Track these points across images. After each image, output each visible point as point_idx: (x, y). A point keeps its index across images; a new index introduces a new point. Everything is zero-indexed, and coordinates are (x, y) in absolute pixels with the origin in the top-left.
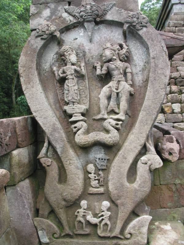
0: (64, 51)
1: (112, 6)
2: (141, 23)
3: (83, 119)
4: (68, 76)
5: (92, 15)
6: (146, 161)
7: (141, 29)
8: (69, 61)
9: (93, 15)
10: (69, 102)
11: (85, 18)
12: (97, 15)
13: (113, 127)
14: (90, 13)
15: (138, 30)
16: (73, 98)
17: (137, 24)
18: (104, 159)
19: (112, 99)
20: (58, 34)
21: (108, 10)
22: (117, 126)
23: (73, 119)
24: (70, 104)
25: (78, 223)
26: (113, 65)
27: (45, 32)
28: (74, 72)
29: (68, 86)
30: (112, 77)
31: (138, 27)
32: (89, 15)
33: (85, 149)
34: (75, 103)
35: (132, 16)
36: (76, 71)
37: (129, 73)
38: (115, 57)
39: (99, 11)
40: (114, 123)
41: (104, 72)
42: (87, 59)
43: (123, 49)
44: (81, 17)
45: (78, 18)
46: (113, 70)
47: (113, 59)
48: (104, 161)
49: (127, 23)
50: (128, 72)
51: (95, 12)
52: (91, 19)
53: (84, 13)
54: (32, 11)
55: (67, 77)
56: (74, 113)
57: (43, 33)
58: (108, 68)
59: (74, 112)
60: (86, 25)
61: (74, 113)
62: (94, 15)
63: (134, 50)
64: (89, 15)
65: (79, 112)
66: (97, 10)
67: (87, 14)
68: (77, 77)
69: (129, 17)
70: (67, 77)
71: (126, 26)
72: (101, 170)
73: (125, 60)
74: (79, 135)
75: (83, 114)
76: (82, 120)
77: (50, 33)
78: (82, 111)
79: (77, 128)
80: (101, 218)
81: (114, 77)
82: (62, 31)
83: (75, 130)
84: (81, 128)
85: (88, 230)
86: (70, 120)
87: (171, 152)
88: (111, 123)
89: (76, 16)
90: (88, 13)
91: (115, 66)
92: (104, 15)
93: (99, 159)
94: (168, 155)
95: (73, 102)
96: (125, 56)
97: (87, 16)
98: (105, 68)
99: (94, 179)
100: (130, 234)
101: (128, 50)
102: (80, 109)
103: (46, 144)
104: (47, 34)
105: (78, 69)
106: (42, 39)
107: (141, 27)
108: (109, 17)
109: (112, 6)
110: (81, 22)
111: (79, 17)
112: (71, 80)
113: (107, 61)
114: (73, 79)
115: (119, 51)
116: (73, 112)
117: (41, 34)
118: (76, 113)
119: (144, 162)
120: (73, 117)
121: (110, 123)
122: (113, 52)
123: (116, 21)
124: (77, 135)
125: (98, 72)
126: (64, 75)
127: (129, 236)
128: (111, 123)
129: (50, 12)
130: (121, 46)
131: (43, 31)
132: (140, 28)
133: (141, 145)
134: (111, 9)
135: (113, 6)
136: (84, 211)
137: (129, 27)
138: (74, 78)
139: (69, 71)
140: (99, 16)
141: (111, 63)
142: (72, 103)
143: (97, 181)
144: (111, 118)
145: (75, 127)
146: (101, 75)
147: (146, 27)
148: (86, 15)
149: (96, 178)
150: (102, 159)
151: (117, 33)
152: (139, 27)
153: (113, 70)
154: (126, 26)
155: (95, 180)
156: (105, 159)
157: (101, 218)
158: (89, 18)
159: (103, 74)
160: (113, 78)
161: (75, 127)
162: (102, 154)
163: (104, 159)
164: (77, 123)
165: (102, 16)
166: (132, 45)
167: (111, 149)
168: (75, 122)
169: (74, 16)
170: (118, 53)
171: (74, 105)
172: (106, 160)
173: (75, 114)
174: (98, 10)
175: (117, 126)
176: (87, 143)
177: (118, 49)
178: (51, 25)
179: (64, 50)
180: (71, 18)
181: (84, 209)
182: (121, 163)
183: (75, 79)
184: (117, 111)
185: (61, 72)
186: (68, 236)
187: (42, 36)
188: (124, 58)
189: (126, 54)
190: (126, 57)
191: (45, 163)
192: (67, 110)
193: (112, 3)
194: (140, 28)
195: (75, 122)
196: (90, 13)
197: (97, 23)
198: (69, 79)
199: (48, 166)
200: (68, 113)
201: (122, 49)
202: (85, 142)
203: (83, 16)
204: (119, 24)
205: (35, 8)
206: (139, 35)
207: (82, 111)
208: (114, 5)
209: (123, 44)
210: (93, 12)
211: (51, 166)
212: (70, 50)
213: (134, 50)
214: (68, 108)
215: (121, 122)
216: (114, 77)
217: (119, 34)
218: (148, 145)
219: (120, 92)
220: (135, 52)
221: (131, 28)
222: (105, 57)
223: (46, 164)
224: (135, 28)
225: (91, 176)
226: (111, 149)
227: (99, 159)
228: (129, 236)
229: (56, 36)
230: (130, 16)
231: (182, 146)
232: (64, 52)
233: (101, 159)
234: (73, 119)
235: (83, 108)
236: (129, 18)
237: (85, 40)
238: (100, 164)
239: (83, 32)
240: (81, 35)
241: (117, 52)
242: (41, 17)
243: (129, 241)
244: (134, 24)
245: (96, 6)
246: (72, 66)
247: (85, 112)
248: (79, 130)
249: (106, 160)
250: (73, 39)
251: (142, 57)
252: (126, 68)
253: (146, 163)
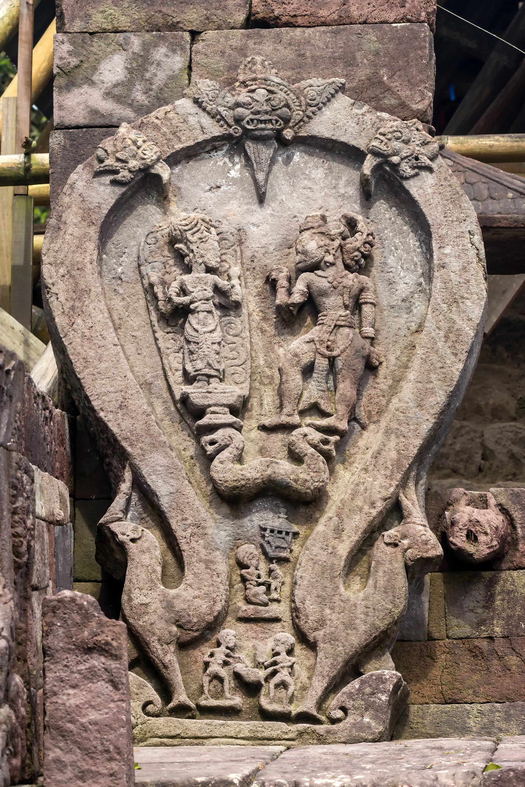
0: (186, 228)
1: (333, 92)
2: (417, 159)
3: (235, 423)
4: (196, 305)
5: (270, 121)
6: (395, 538)
7: (417, 175)
8: (200, 261)
9: (274, 122)
10: (199, 375)
11: (249, 127)
12: (287, 121)
13: (315, 447)
14: (266, 113)
15: (407, 178)
16: (209, 365)
17: (402, 159)
18: (284, 533)
19: (314, 375)
20: (164, 171)
21: (321, 105)
22: (326, 447)
23: (205, 421)
24: (199, 381)
25: (210, 681)
26: (323, 280)
27: (125, 161)
28: (212, 294)
29: (197, 331)
30: (320, 315)
31: (406, 169)
32: (261, 121)
33: (234, 500)
34: (211, 380)
35: (390, 136)
36: (216, 289)
37: (369, 306)
38: (329, 258)
39: (292, 106)
40: (316, 436)
41: (297, 298)
42: (248, 254)
43: (357, 235)
44: (238, 120)
45: (226, 122)
46: (324, 294)
47: (326, 262)
48: (283, 538)
49: (376, 154)
50: (366, 303)
51: (279, 112)
52: (266, 132)
53: (247, 112)
54: (61, 58)
55: (192, 306)
56: (210, 406)
57: (119, 164)
58: (308, 287)
59: (211, 402)
60: (250, 147)
61: (210, 406)
62: (277, 121)
63: (391, 234)
64: (261, 121)
65: (225, 402)
66: (287, 106)
67: (257, 117)
68: (220, 307)
69: (382, 138)
70: (192, 306)
71: (369, 164)
72: (274, 561)
73: (360, 266)
74: (221, 462)
75: (234, 410)
76: (230, 425)
77: (142, 167)
78: (231, 402)
79: (216, 445)
80: (271, 669)
81: (325, 313)
82: (173, 160)
83: (210, 449)
84: (227, 446)
85: (236, 700)
86: (201, 422)
87: (473, 530)
88: (310, 437)
89: (221, 116)
90: (258, 113)
91: (328, 285)
92: (305, 119)
93: (272, 531)
94: (464, 539)
95: (209, 376)
96: (360, 255)
97: (255, 121)
98: (300, 286)
99: (256, 582)
100: (344, 709)
101: (371, 238)
102: (226, 395)
103: (125, 487)
104: (133, 169)
105: (222, 283)
106: (114, 182)
107: (416, 170)
108: (321, 126)
109: (333, 92)
110: (237, 137)
111: (231, 121)
112: (205, 313)
113: (306, 266)
114: (210, 312)
115: (344, 239)
116: (207, 403)
117: (114, 168)
118: (215, 405)
119: (392, 541)
120: (208, 416)
121: (306, 435)
122: (328, 241)
123: (342, 142)
124: (216, 462)
125: (281, 298)
126: (185, 299)
127: (339, 714)
128: (310, 437)
129: (127, 68)
130: (351, 224)
131: (118, 160)
132: (412, 172)
133: (385, 500)
134: (329, 100)
135: (337, 92)
136: (228, 651)
137: (377, 168)
138: (214, 309)
139: (199, 288)
140: (291, 124)
141: (319, 272)
142: (205, 378)
143: (263, 588)
144: (309, 425)
145: (212, 443)
146: (288, 306)
147: (430, 169)
148: (252, 120)
149: (260, 581)
150: (280, 532)
151: (344, 178)
152: (409, 170)
153: (324, 294)
154: (369, 164)
155: (259, 584)
156: (287, 533)
157: (271, 669)
158: (263, 129)
159: (294, 305)
160: (322, 318)
161: (212, 443)
162: (281, 520)
163: (284, 533)
164: (217, 432)
165: (302, 123)
166: (386, 219)
167: (303, 504)
168: (213, 428)
169: (214, 115)
170: (341, 247)
171: (209, 384)
172: (291, 534)
173: (212, 409)
174: (290, 102)
175: (326, 447)
176: (243, 482)
177: (341, 234)
178: (144, 141)
179: (187, 225)
180: (206, 120)
181: (227, 648)
182: (327, 539)
183: (214, 311)
184: (324, 406)
185: (177, 290)
186: (181, 711)
187: (116, 172)
188: (357, 262)
189: (362, 250)
190: (364, 256)
191: (124, 534)
192: (193, 395)
193: (334, 82)
194: (412, 172)
195: (213, 428)
196: (266, 113)
197: (284, 144)
198: (198, 312)
199: (133, 540)
200: (192, 403)
201: (353, 235)
202: (236, 480)
203: (243, 120)
204: (352, 155)
205: (71, 48)
206: (407, 193)
207: (231, 400)
208: (340, 88)
209: (356, 220)
210: (273, 110)
211: (139, 542)
212: (203, 227)
213: (391, 234)
214: (193, 391)
215: (334, 439)
216: (325, 313)
217: (348, 183)
218: (406, 502)
219: (339, 356)
220: (394, 242)
221: (386, 171)
222: (303, 254)
223: (128, 536)
224: (397, 171)
225: (248, 573)
226: (303, 504)
227: (272, 531)
228: (339, 714)
229: (158, 177)
230: (384, 135)
231: (522, 531)
232: (185, 231)
233: (276, 532)
234: (205, 421)
235: (236, 394)
236: (382, 141)
237: (245, 194)
238: (272, 543)
239: (238, 167)
240: (233, 178)
241: (337, 243)
242: (92, 83)
243: (341, 724)
244: (395, 159)
245: (286, 89)
246: (208, 274)
247: (238, 405)
248: (219, 451)
249: (291, 534)
250: (208, 188)
251: (412, 260)
252: (362, 290)
253: (396, 545)
